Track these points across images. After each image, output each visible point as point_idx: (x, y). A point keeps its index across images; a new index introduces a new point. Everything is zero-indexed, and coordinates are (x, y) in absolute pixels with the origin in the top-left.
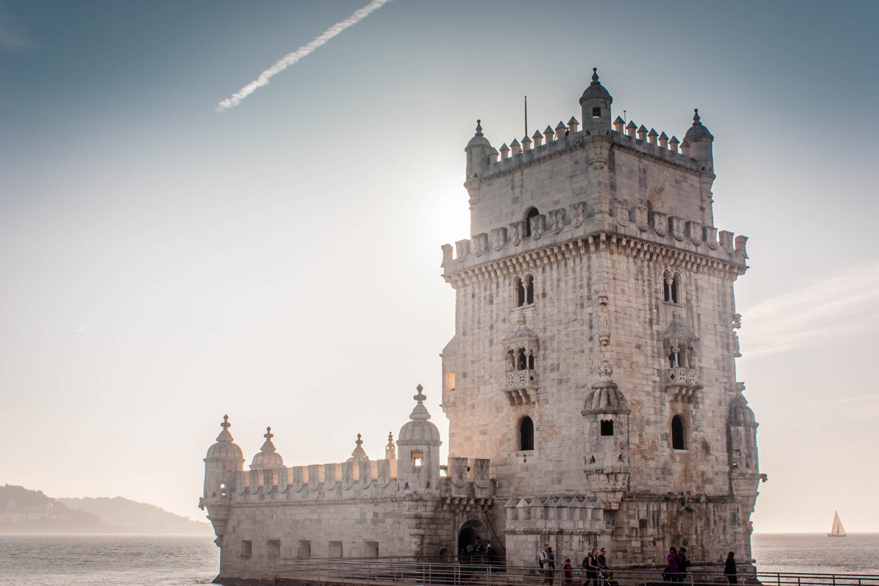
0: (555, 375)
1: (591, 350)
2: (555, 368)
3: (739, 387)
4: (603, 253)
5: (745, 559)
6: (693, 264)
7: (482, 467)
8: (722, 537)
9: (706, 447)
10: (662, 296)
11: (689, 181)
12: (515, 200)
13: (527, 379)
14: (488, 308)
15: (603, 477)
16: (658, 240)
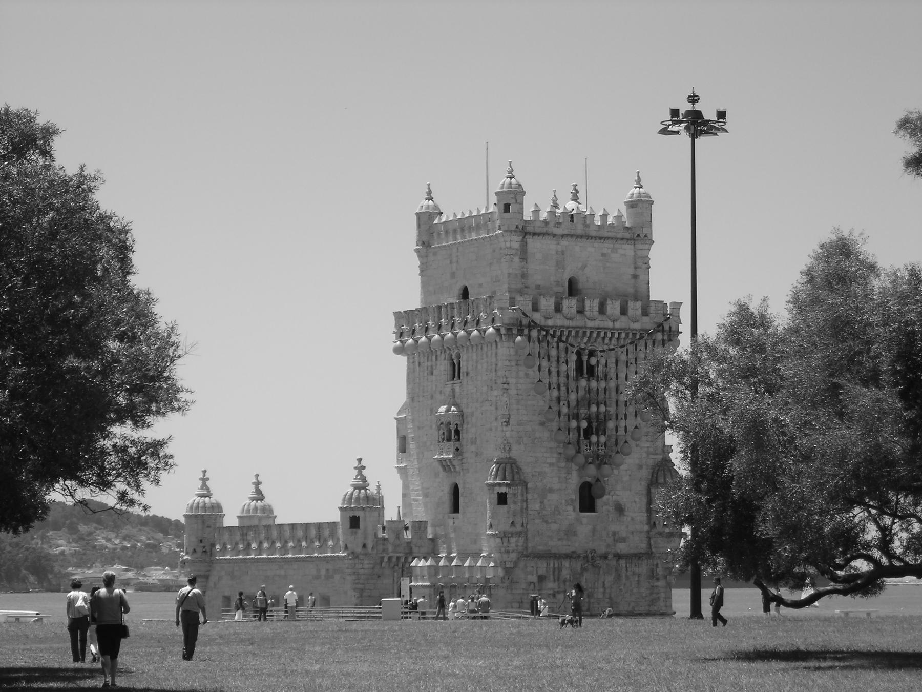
0: (473, 448)
1: (496, 428)
2: (474, 442)
3: (666, 449)
4: (506, 344)
5: (664, 609)
6: (610, 339)
7: (420, 528)
8: (635, 590)
9: (620, 509)
10: (572, 374)
11: (621, 251)
12: (453, 275)
13: (453, 449)
14: (429, 377)
15: (498, 540)
16: (567, 323)
